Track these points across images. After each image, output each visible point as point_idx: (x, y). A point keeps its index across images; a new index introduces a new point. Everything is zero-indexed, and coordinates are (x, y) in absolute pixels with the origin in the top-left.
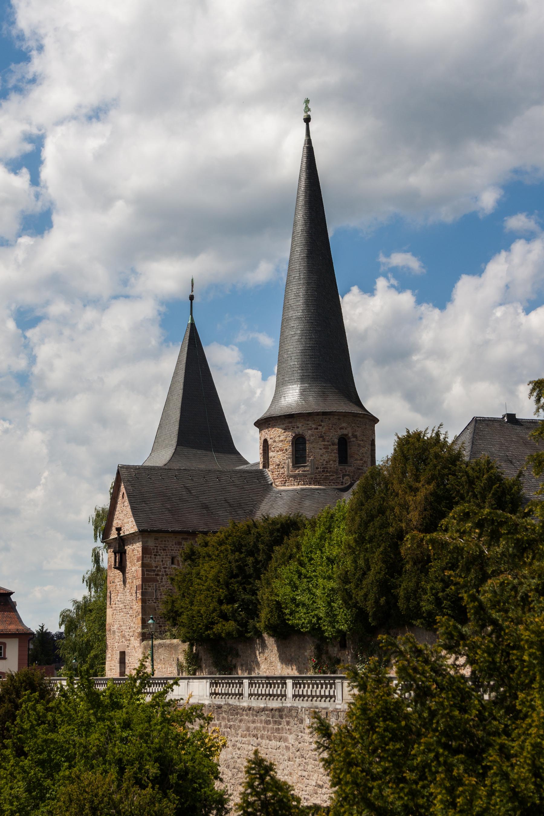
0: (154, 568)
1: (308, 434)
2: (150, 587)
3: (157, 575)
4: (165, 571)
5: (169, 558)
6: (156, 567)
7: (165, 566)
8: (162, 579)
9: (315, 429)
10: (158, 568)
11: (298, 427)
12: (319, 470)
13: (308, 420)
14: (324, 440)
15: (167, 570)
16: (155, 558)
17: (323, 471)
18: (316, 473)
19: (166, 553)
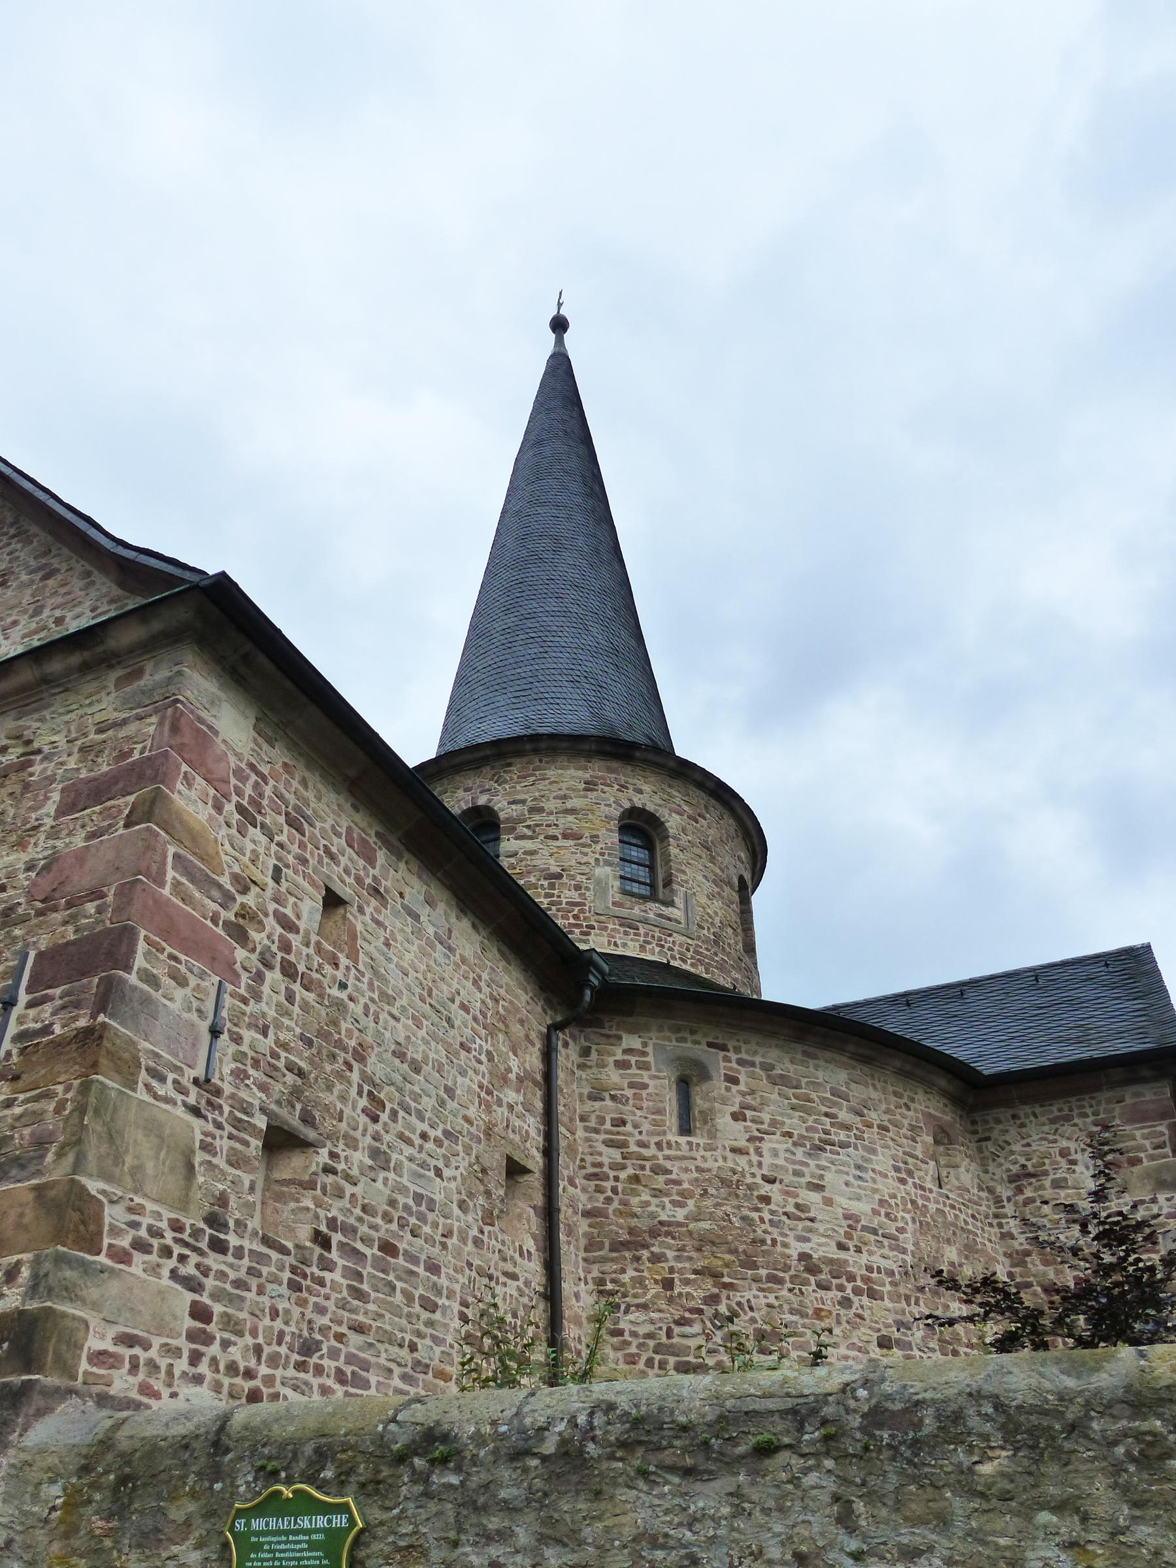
0: (225, 881)
1: (673, 822)
2: (182, 982)
3: (240, 935)
4: (286, 947)
5: (313, 883)
6: (244, 884)
7: (288, 911)
8: (259, 977)
9: (689, 817)
10: (250, 900)
11: (640, 792)
12: (705, 932)
13: (670, 786)
14: (712, 860)
15: (295, 940)
16: (242, 832)
17: (715, 941)
18: (699, 938)
19: (302, 845)
